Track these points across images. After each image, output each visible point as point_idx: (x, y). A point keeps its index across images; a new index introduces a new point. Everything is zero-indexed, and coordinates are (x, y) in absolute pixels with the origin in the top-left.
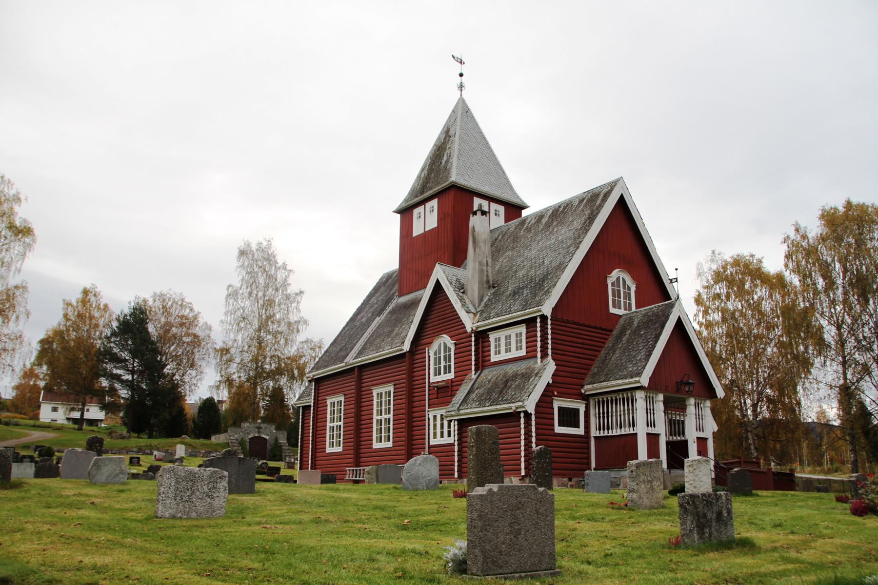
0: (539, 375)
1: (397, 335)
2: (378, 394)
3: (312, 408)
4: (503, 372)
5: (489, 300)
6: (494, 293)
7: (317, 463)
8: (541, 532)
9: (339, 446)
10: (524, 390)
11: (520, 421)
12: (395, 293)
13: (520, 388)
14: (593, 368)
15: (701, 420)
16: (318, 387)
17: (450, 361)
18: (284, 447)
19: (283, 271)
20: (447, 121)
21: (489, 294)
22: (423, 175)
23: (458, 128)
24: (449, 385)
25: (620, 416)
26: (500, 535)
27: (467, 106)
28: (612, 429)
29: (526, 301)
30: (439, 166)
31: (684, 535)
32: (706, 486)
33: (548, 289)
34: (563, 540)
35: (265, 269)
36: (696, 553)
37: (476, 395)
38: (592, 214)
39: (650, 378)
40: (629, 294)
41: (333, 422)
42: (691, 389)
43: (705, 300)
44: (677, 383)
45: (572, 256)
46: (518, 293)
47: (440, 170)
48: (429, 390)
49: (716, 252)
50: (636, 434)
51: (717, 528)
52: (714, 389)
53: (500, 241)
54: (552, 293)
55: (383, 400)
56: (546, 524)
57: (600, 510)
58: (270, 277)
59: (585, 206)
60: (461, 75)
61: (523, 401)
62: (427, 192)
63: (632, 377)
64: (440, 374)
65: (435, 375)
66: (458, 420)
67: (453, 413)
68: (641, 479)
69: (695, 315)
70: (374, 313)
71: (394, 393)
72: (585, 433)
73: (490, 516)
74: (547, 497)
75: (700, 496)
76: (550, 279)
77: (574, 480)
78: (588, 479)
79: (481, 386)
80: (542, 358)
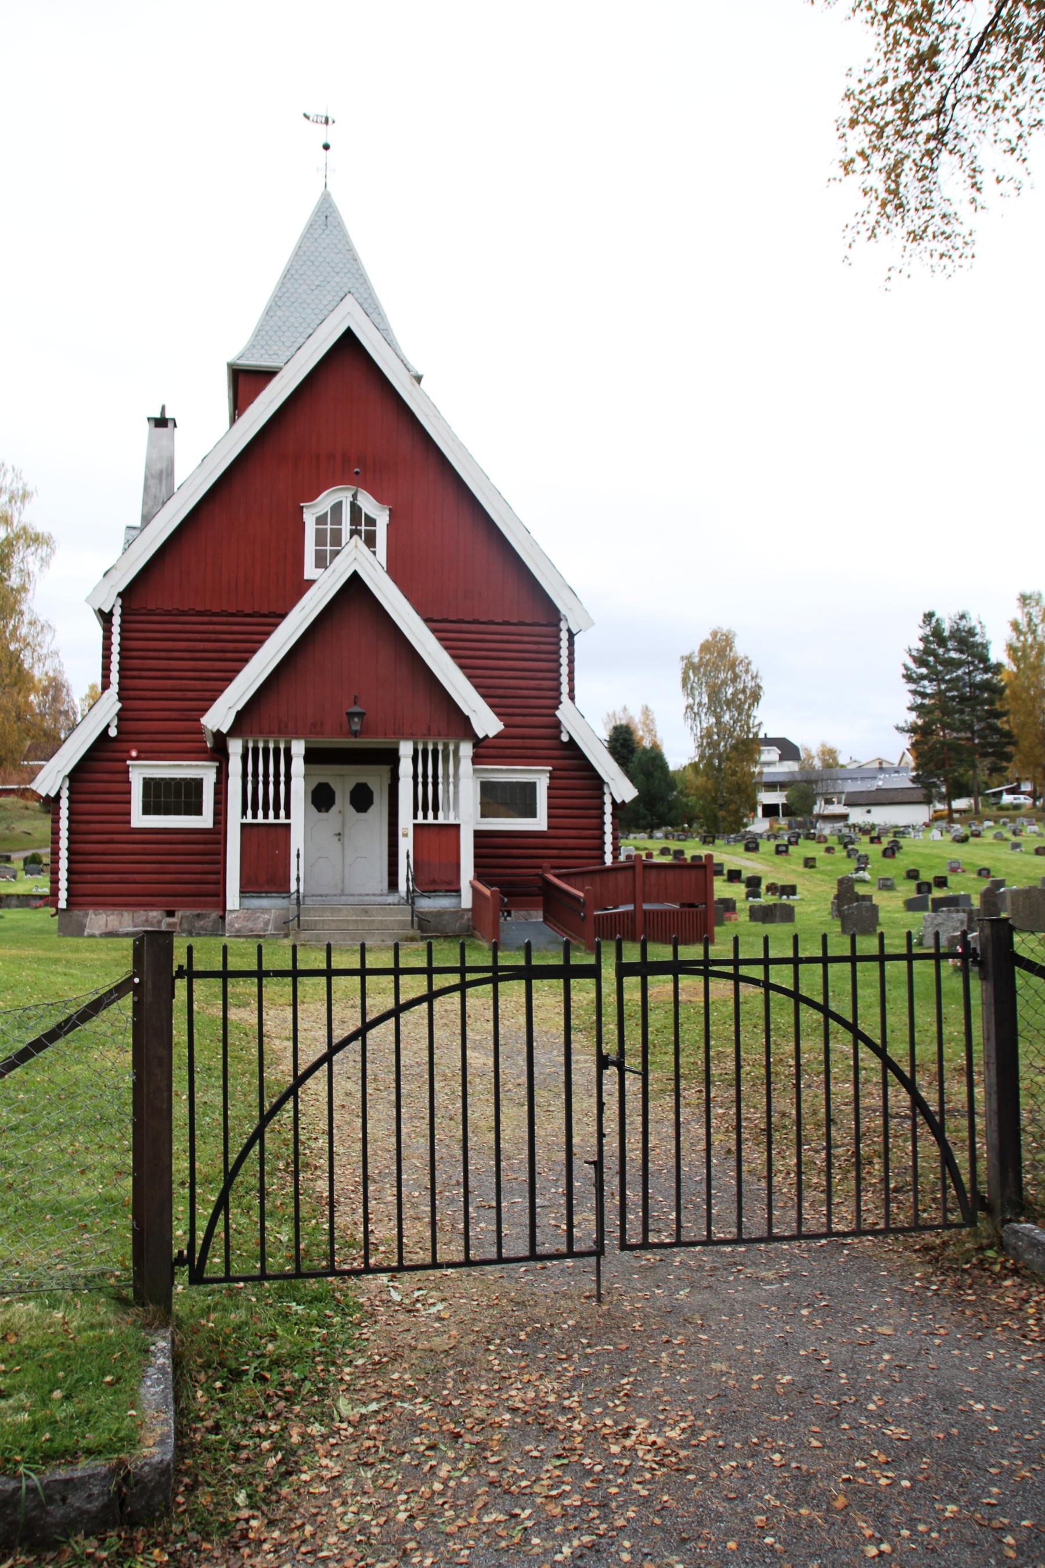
72: (215, 822)
77: (179, 914)
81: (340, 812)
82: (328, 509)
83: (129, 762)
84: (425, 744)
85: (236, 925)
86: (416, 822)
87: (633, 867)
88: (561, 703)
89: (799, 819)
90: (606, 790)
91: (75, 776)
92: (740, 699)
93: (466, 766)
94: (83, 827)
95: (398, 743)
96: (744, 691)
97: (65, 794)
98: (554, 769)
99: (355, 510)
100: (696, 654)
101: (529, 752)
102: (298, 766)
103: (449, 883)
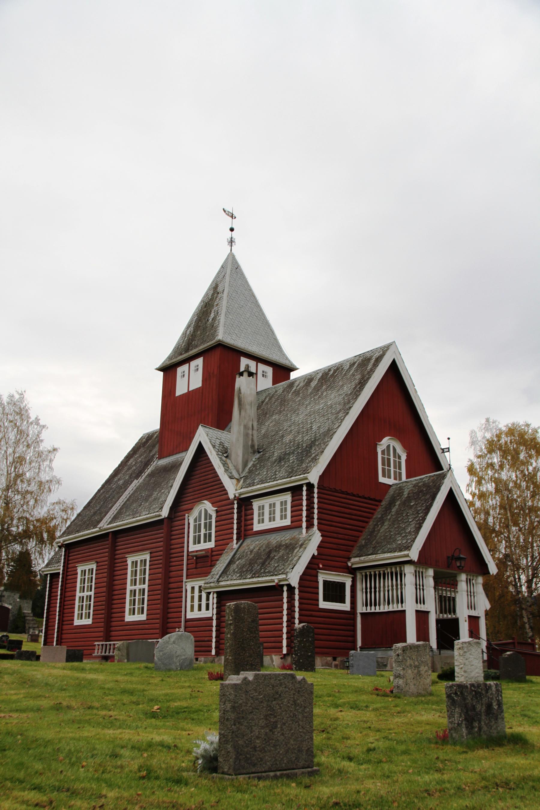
0: (304, 546)
1: (155, 499)
2: (133, 562)
3: (61, 576)
4: (266, 542)
5: (254, 465)
6: (258, 458)
7: (64, 636)
8: (299, 725)
9: (89, 618)
10: (287, 561)
11: (282, 595)
12: (154, 455)
13: (284, 560)
14: (360, 539)
15: (472, 597)
16: (69, 553)
17: (210, 529)
18: (28, 618)
19: (36, 427)
20: (216, 277)
21: (254, 460)
22: (188, 332)
23: (227, 285)
24: (209, 554)
25: (388, 591)
26: (254, 728)
27: (237, 262)
28: (379, 605)
29: (292, 468)
30: (206, 323)
31: (452, 729)
32: (477, 670)
33: (315, 456)
34: (323, 731)
35: (16, 424)
36: (465, 750)
37: (237, 565)
38: (363, 378)
39: (420, 552)
40: (400, 463)
41: (84, 592)
42: (463, 565)
43: (478, 470)
44: (448, 557)
45: (341, 422)
46: (284, 459)
47: (207, 327)
48: (188, 560)
49: (491, 420)
50: (404, 611)
51: (487, 722)
52: (486, 565)
53: (267, 403)
54: (320, 460)
55: (138, 568)
56: (304, 717)
57: (364, 697)
58: (21, 432)
59: (356, 370)
60: (232, 230)
61: (286, 574)
62: (192, 350)
63: (401, 551)
64: (199, 542)
65: (195, 543)
66: (218, 593)
67: (212, 585)
68: (408, 664)
69: (468, 485)
70: (131, 474)
71: (150, 561)
72: (351, 608)
73: (244, 708)
74: (306, 686)
75: (469, 686)
76: (317, 445)
77: (339, 659)
78: (352, 660)
79: (243, 556)
80: (308, 528)
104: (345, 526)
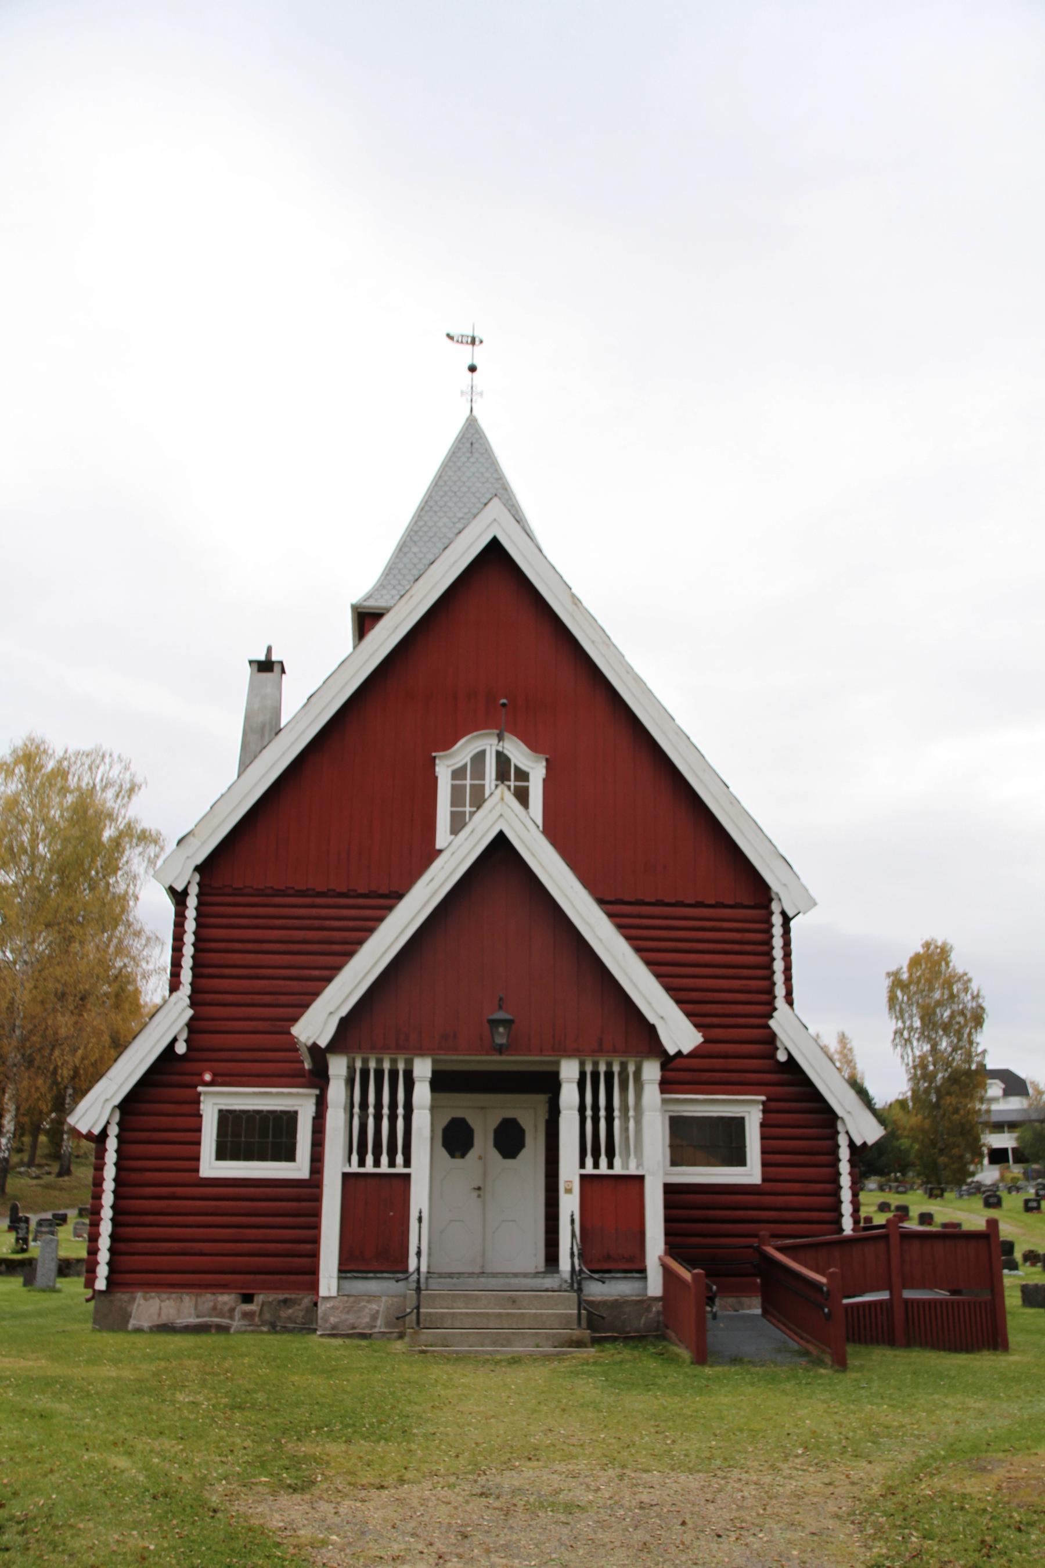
52: (652, 1029)
77: (259, 1298)
81: (480, 1158)
82: (468, 759)
83: (200, 1089)
84: (596, 1064)
85: (333, 1320)
86: (584, 1172)
87: (885, 1237)
88: (775, 1009)
89: (1035, 1166)
90: (840, 1127)
91: (129, 1106)
92: (959, 1023)
93: (652, 1094)
94: (135, 1177)
95: (558, 1063)
96: (962, 1013)
97: (113, 1131)
98: (769, 1100)
99: (503, 760)
100: (905, 969)
101: (734, 1076)
102: (422, 1093)
103: (630, 1259)
104: (306, 972)
